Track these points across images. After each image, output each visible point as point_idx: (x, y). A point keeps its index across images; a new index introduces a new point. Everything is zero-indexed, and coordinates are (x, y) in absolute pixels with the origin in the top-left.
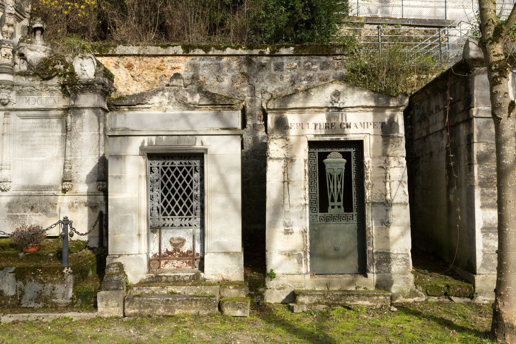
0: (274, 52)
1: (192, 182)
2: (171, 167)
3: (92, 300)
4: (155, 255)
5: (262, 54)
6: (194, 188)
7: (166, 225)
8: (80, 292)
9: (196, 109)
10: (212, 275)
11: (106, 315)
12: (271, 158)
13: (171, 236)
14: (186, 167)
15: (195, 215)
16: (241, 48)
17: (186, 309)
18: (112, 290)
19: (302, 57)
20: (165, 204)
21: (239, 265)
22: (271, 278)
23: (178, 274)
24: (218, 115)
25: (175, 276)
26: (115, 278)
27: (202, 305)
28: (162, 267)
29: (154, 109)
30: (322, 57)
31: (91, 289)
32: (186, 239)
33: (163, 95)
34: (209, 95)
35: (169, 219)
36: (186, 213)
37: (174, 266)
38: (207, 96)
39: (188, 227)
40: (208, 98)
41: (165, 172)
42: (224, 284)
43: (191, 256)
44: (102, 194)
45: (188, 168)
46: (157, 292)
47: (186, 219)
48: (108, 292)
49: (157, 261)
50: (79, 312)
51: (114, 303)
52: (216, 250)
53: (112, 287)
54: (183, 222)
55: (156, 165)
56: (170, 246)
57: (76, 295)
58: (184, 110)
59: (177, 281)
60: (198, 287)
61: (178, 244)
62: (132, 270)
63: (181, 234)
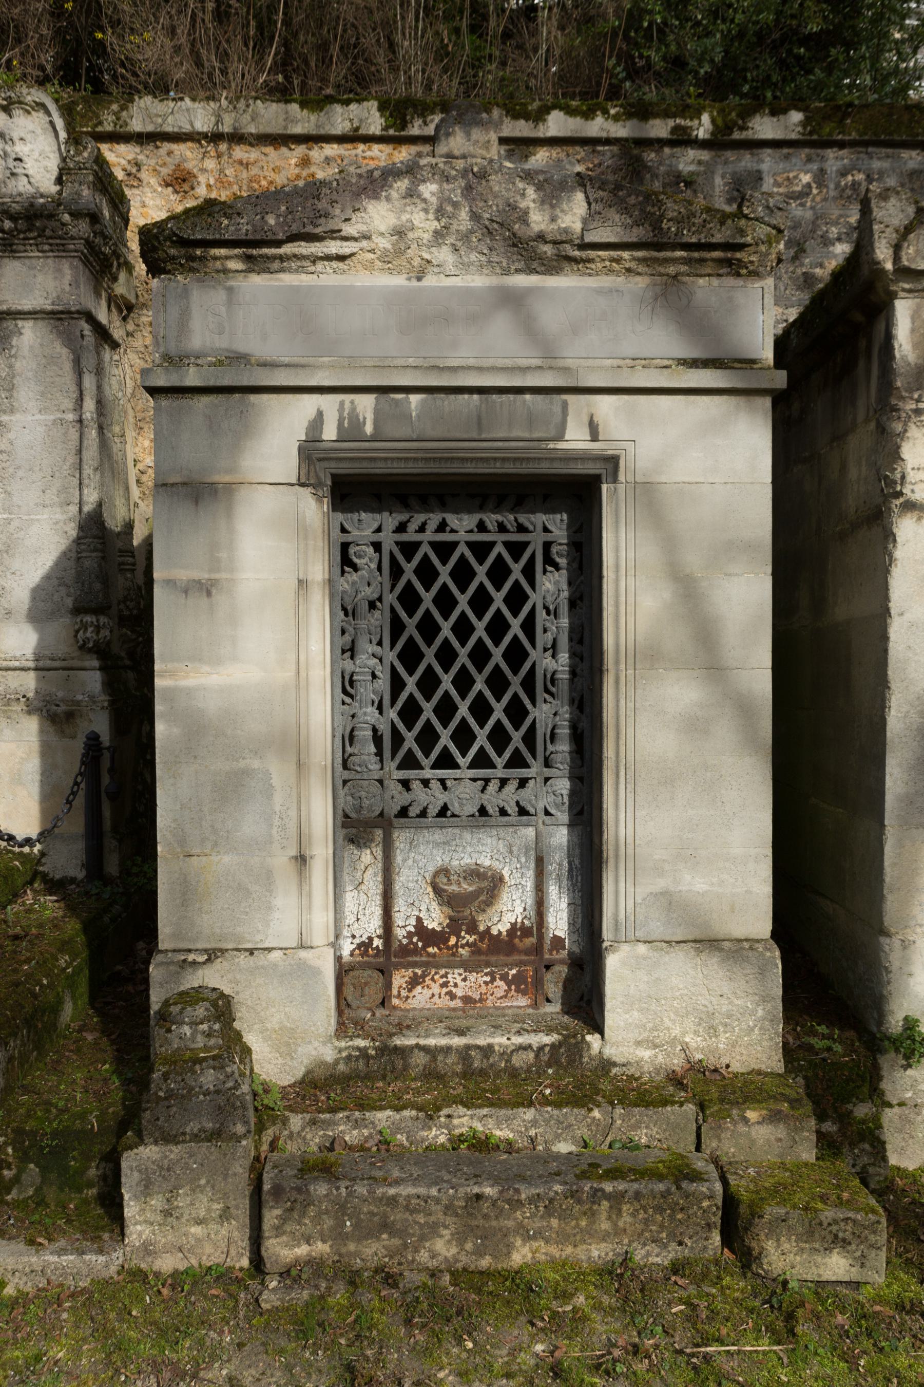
0: (729, 128)
1: (532, 613)
2: (433, 544)
3: (92, 1172)
4: (365, 946)
5: (682, 139)
6: (543, 639)
7: (414, 811)
8: (33, 1133)
9: (567, 266)
10: (638, 1043)
11: (167, 1264)
12: (910, 506)
13: (439, 859)
14: (507, 544)
15: (547, 764)
16: (605, 112)
17: (563, 1238)
18: (196, 1138)
19: (831, 153)
20: (410, 713)
21: (764, 999)
22: (907, 1057)
23: (482, 1041)
24: (670, 297)
25: (468, 1047)
26: (209, 1078)
27: (646, 1222)
28: (395, 1001)
29: (369, 267)
30: (905, 154)
31: (83, 1116)
32: (506, 873)
33: (411, 194)
34: (632, 200)
35: (426, 783)
36: (507, 754)
37: (452, 996)
38: (622, 201)
39: (514, 819)
40: (626, 210)
41: (409, 568)
42: (705, 1089)
43: (527, 952)
44: (96, 663)
45: (516, 549)
46: (401, 1138)
47: (504, 782)
48: (174, 1152)
49: (376, 974)
50: (31, 1242)
51: (205, 1204)
52: (657, 928)
53: (193, 1127)
54: (492, 798)
55: (368, 532)
56: (434, 905)
57: (13, 1144)
58: (506, 272)
59: (485, 1080)
60: (596, 1113)
61: (467, 897)
62: (273, 1023)
63: (482, 850)
